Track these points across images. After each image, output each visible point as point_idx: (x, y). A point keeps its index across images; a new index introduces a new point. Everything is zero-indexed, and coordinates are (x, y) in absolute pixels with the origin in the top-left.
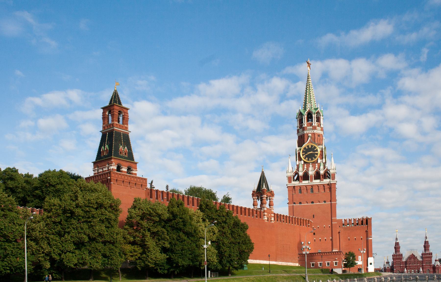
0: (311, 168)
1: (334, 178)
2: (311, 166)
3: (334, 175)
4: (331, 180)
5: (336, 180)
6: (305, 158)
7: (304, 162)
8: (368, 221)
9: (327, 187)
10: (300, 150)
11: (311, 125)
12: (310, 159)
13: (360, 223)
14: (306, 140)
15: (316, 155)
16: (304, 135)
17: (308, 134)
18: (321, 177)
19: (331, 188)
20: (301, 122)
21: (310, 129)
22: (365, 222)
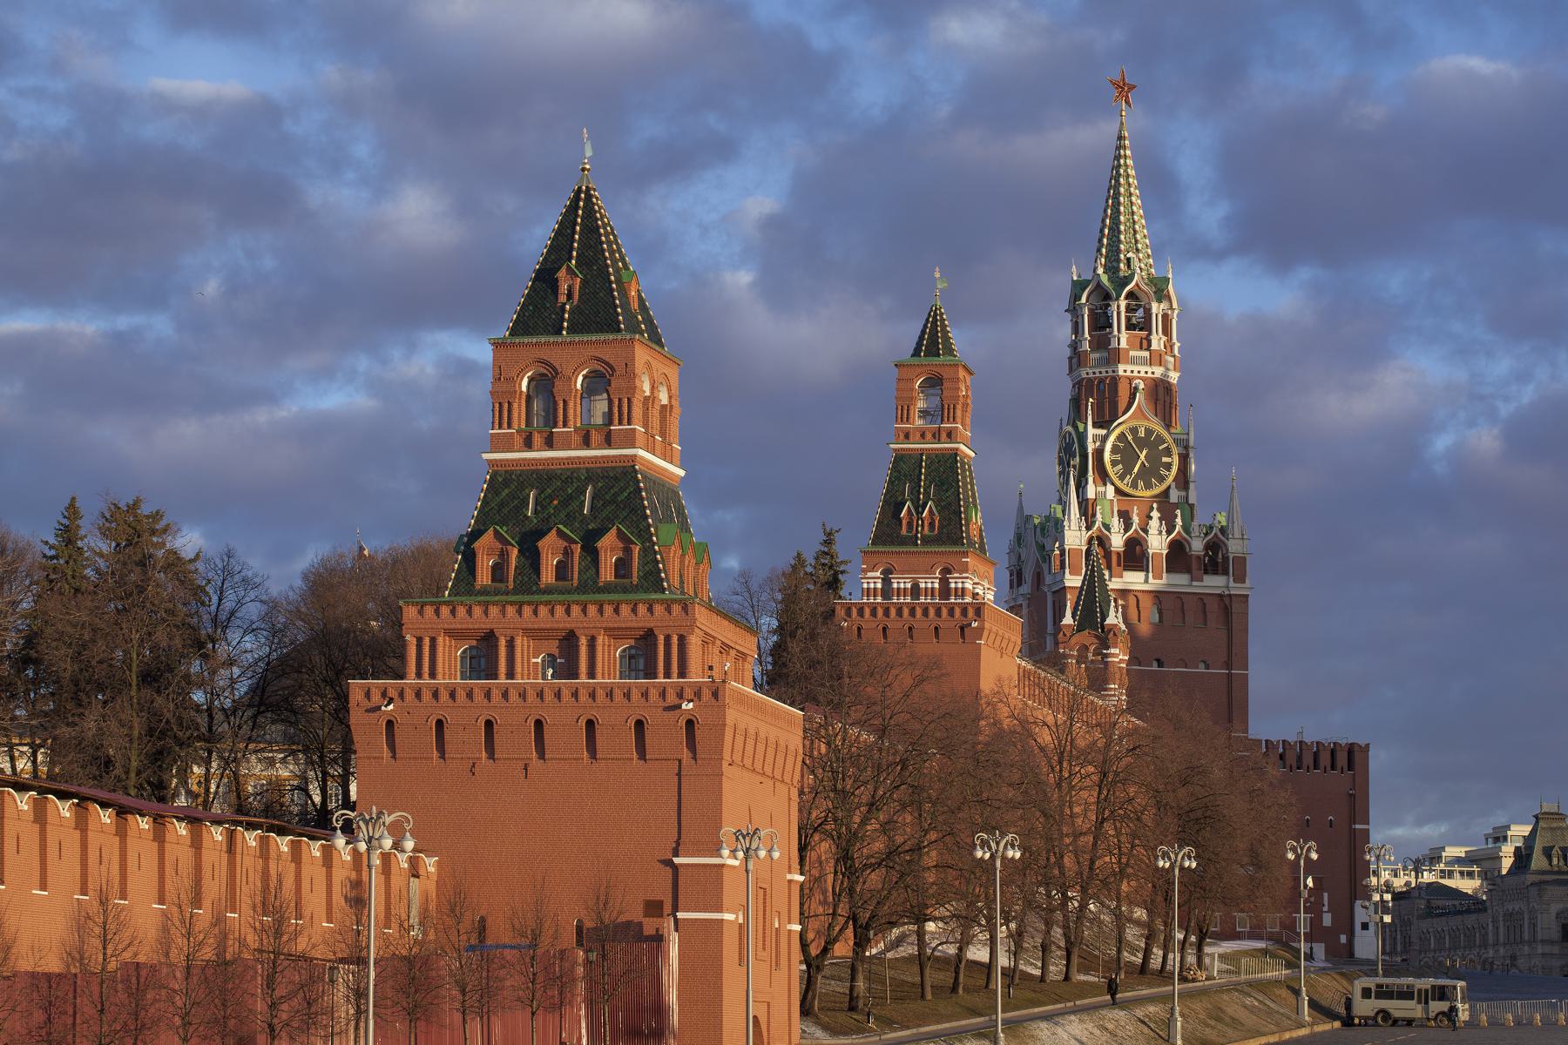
0: (1154, 524)
1: (1240, 578)
2: (1155, 514)
3: (1241, 562)
4: (1232, 584)
5: (1248, 584)
6: (1122, 478)
7: (1118, 491)
8: (1357, 757)
9: (1213, 606)
10: (1104, 439)
11: (1145, 344)
12: (1141, 484)
13: (1308, 760)
14: (1122, 406)
15: (1163, 472)
16: (1115, 380)
17: (1130, 380)
18: (1194, 565)
19: (1229, 611)
20: (1101, 323)
21: (1143, 362)
22: (1342, 759)
